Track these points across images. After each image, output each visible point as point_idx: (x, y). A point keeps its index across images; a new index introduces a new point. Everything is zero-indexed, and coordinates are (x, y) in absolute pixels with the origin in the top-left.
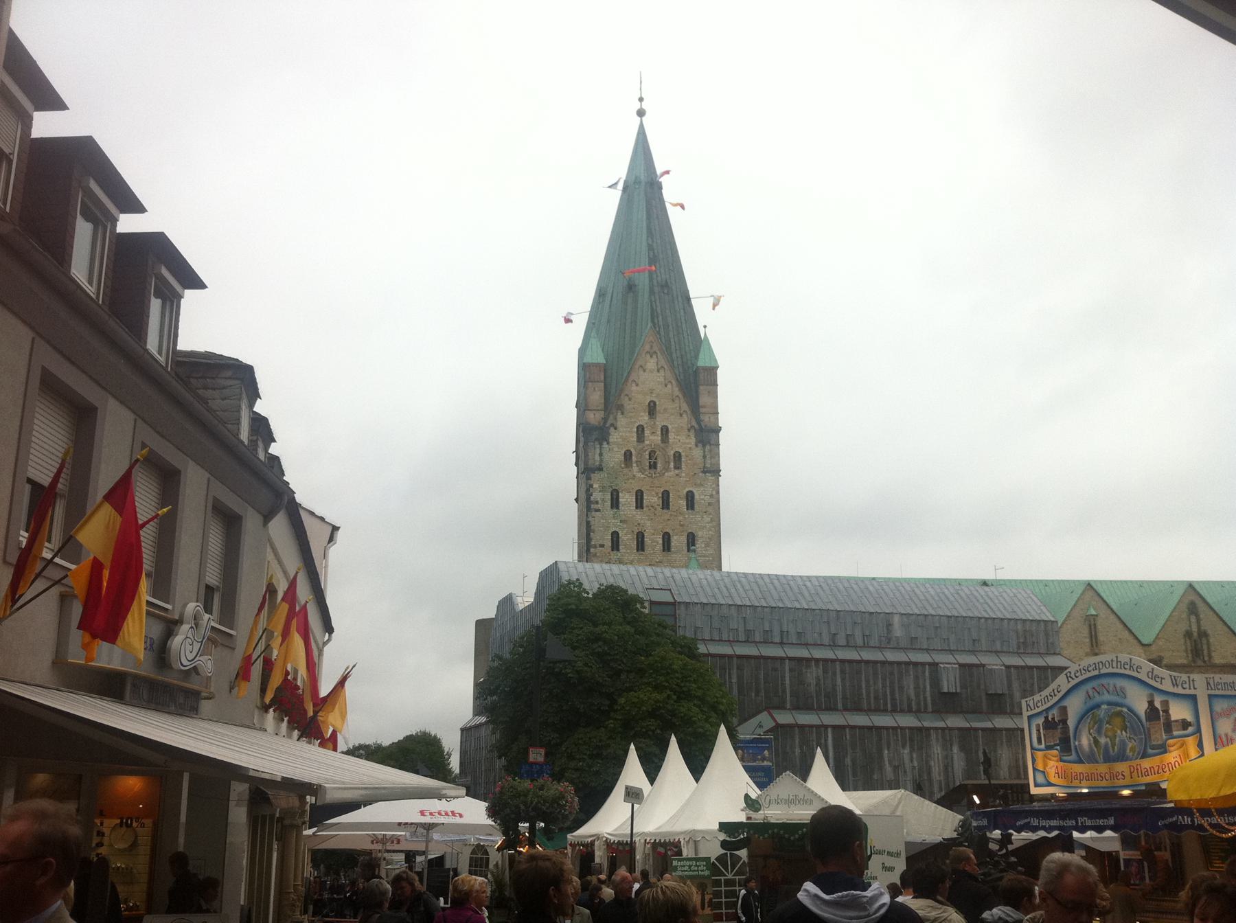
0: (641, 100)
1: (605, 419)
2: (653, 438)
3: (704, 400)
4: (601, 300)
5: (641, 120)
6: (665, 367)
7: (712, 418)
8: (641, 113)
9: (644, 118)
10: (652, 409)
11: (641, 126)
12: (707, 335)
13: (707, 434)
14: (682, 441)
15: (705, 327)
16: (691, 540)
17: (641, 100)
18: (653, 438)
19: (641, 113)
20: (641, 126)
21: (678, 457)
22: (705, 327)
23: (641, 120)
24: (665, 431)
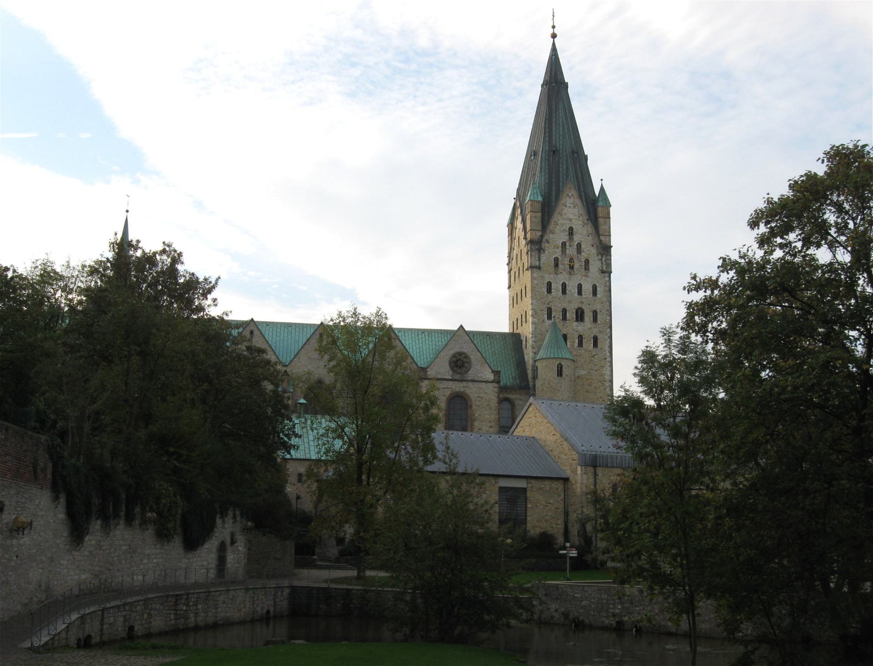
0: (554, 27)
1: (542, 236)
2: (571, 251)
3: (602, 228)
4: (533, 158)
5: (554, 41)
6: (579, 204)
7: (607, 239)
8: (554, 36)
9: (555, 39)
10: (571, 232)
11: (554, 44)
12: (604, 186)
13: (605, 250)
14: (590, 251)
15: (602, 180)
16: (595, 313)
17: (554, 27)
18: (571, 251)
19: (554, 36)
20: (554, 44)
21: (587, 262)
22: (602, 180)
23: (554, 41)
24: (579, 246)
